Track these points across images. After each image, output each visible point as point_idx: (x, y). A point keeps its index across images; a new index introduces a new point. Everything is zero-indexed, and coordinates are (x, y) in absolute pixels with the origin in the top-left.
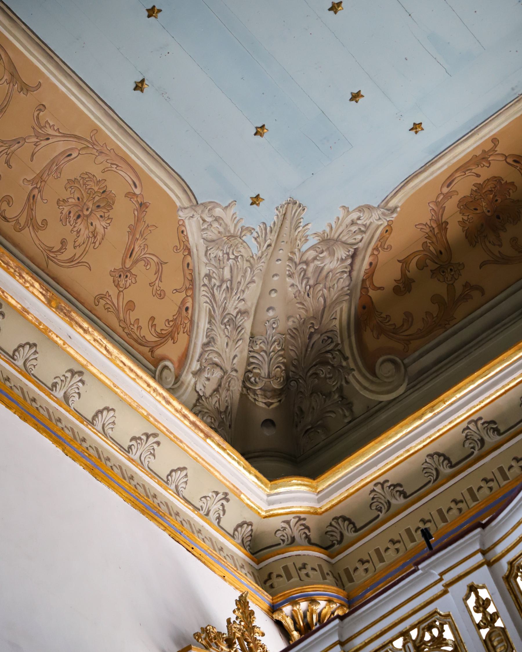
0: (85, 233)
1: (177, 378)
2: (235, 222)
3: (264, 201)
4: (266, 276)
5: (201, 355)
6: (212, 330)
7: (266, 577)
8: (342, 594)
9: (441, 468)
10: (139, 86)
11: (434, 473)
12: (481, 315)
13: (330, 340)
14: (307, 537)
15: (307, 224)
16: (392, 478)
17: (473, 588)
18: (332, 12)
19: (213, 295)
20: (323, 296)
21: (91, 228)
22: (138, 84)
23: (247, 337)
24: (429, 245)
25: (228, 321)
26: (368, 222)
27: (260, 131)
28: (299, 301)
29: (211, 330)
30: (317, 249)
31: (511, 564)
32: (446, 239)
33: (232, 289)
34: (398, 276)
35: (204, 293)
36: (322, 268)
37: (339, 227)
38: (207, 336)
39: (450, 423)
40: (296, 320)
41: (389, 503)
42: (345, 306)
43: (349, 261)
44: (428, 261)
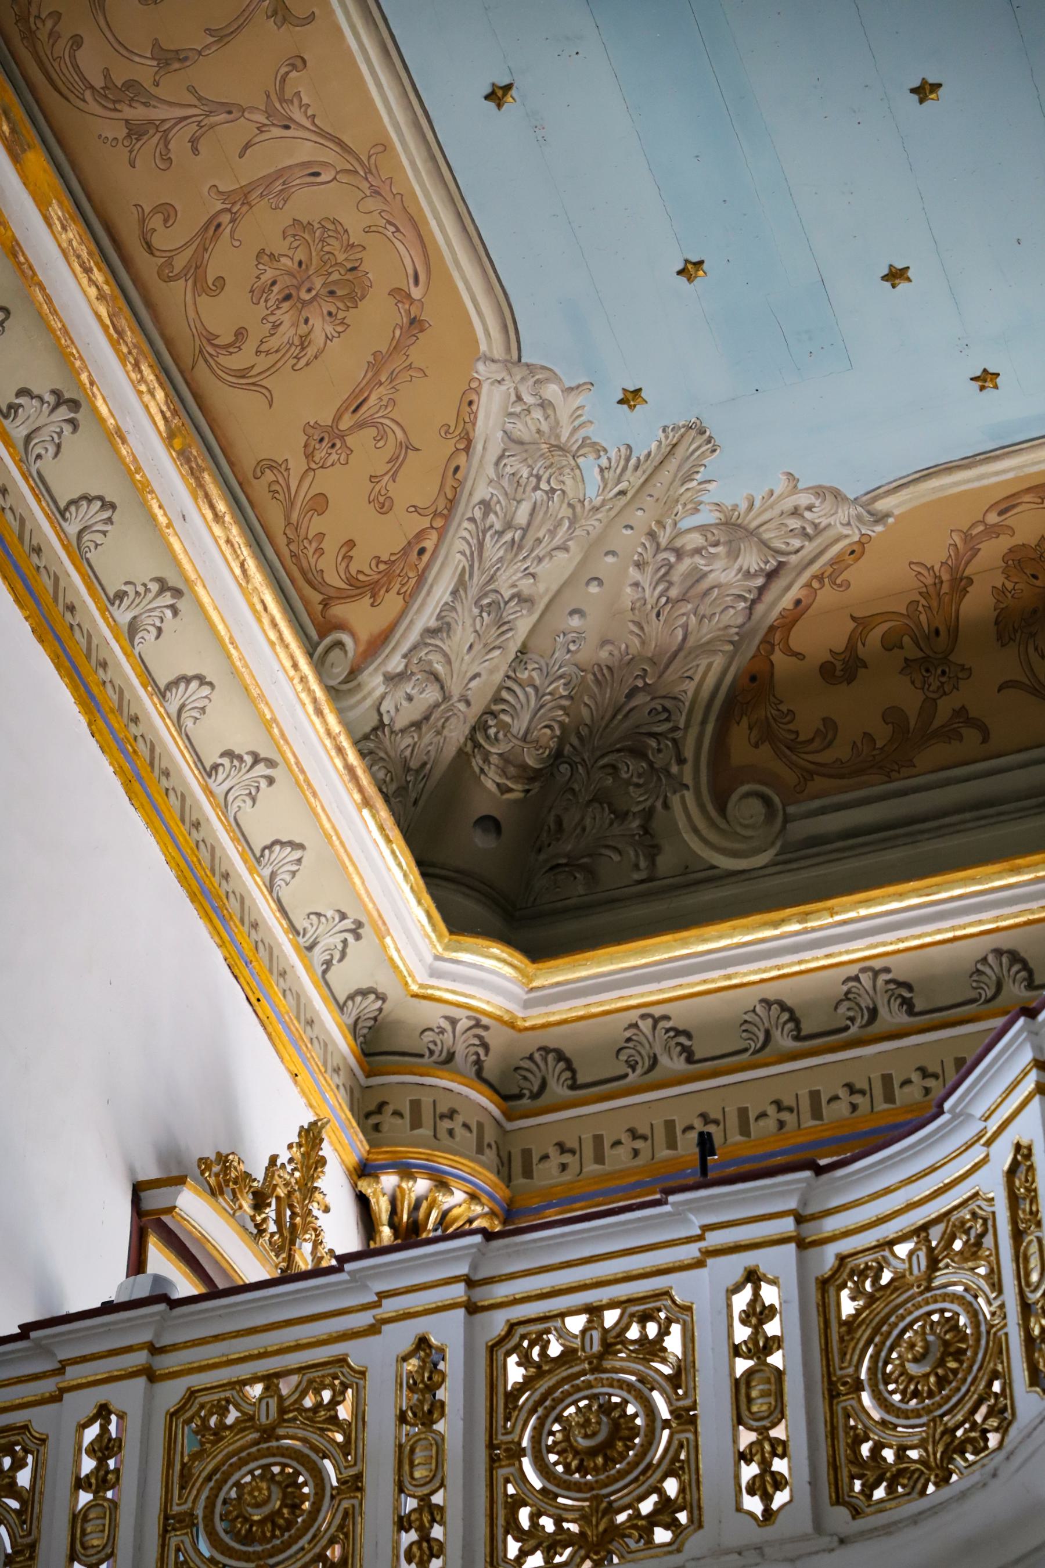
0: (287, 332)
1: (353, 673)
2: (576, 423)
3: (645, 406)
4: (595, 547)
5: (415, 648)
6: (454, 609)
7: (372, 1107)
8: (502, 1192)
9: (777, 1034)
10: (498, 95)
11: (761, 1036)
12: (967, 779)
13: (665, 715)
14: (478, 1062)
15: (709, 481)
16: (680, 1015)
17: (753, 1277)
18: (915, 98)
19: (481, 545)
20: (685, 627)
21: (303, 329)
22: (497, 90)
23: (513, 648)
24: (920, 608)
25: (490, 605)
26: (824, 522)
27: (690, 270)
28: (636, 619)
29: (451, 608)
30: (709, 535)
31: (842, 1259)
32: (958, 611)
33: (520, 547)
34: (840, 645)
35: (466, 534)
36: (705, 575)
37: (766, 510)
38: (439, 617)
39: (827, 956)
40: (616, 652)
41: (654, 1061)
42: (718, 662)
43: (760, 581)
44: (906, 639)
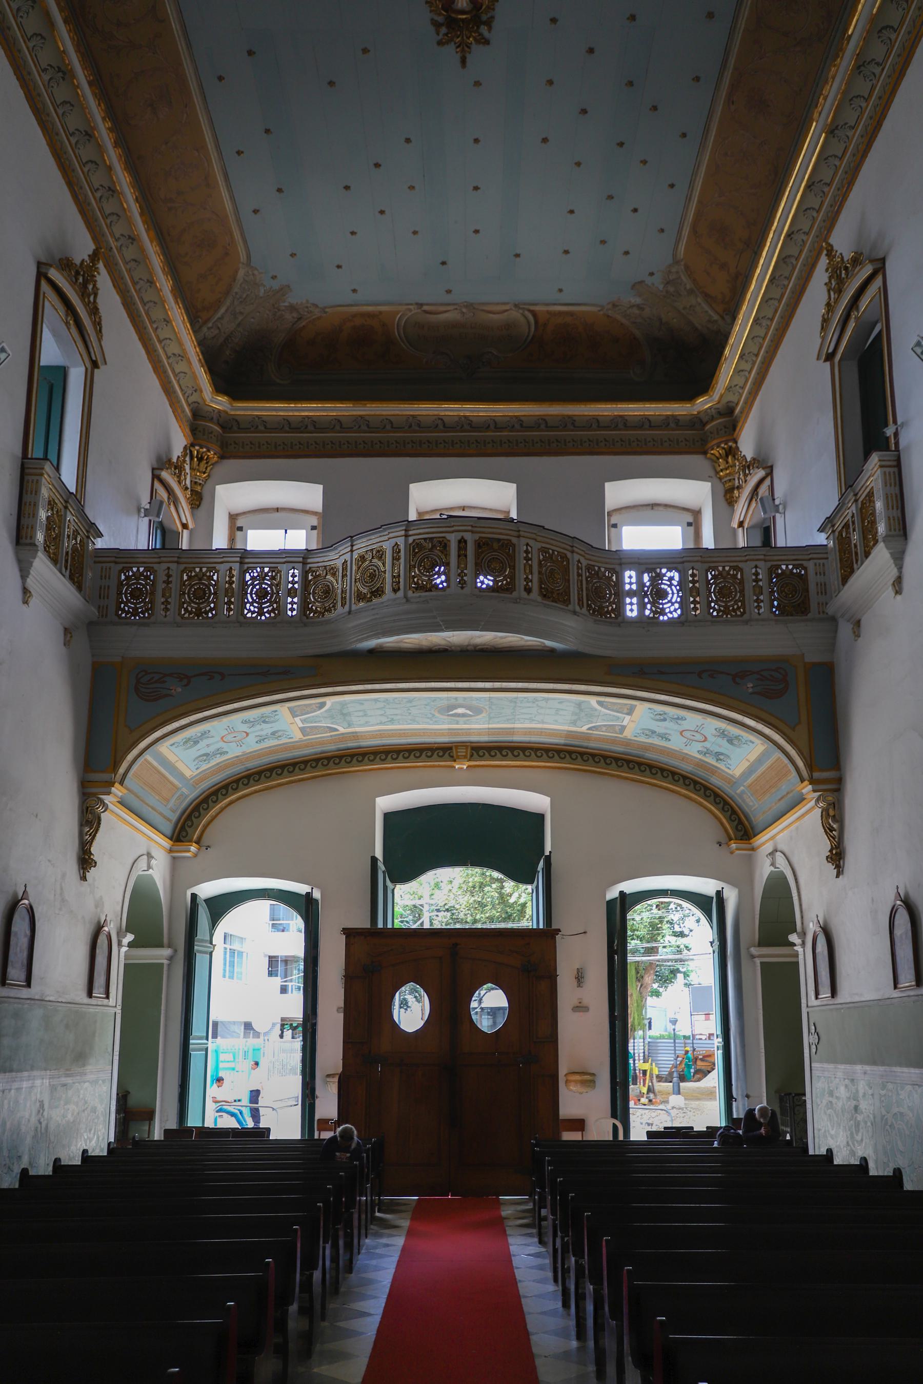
1: (200, 327)
31: (310, 568)
41: (257, 427)
